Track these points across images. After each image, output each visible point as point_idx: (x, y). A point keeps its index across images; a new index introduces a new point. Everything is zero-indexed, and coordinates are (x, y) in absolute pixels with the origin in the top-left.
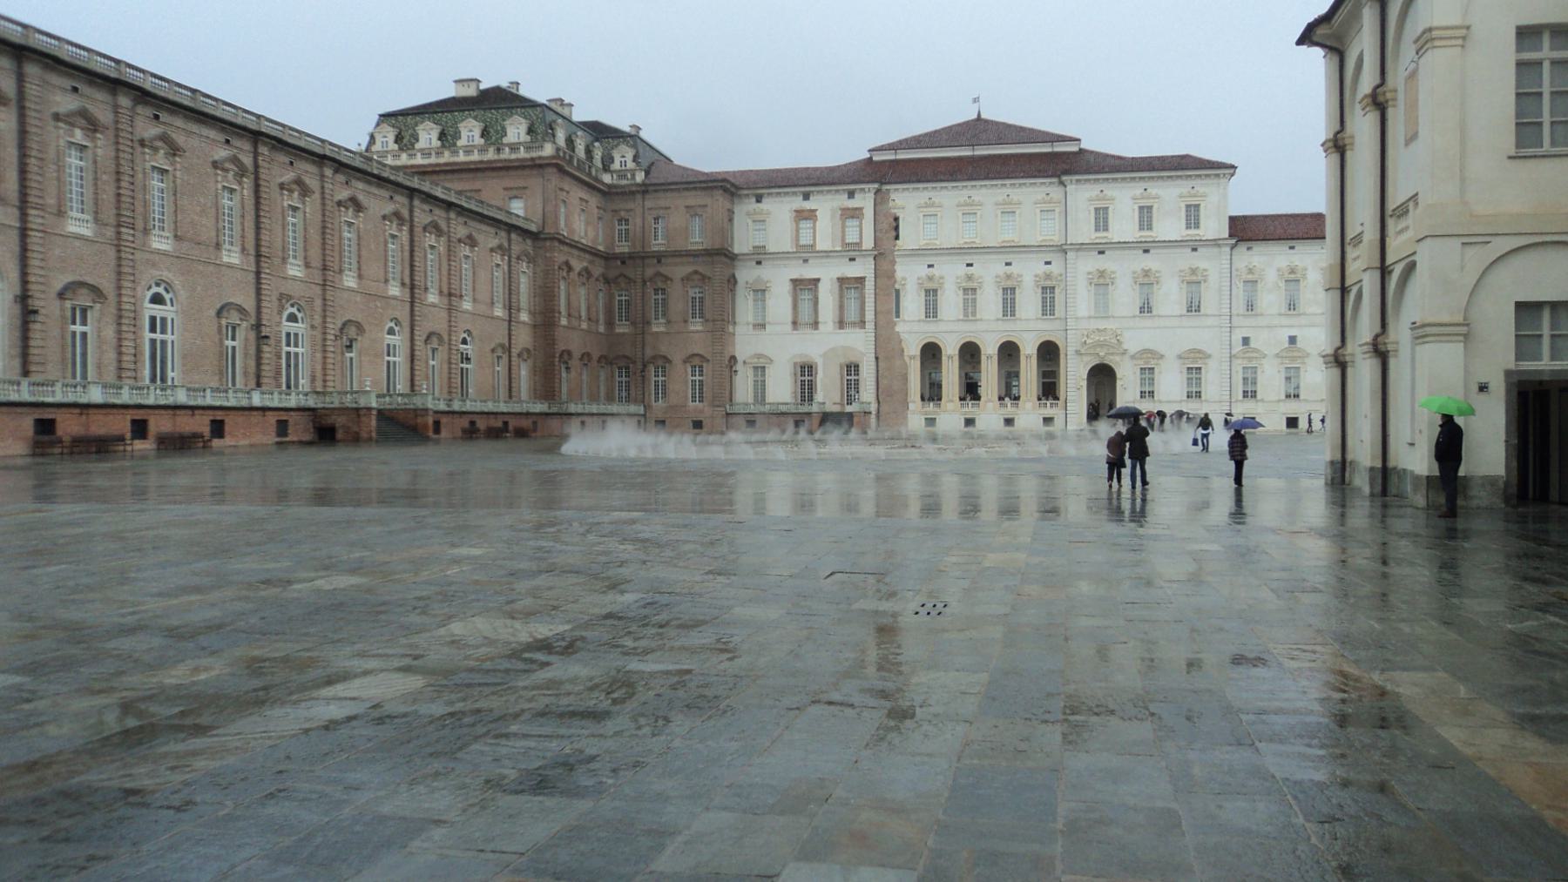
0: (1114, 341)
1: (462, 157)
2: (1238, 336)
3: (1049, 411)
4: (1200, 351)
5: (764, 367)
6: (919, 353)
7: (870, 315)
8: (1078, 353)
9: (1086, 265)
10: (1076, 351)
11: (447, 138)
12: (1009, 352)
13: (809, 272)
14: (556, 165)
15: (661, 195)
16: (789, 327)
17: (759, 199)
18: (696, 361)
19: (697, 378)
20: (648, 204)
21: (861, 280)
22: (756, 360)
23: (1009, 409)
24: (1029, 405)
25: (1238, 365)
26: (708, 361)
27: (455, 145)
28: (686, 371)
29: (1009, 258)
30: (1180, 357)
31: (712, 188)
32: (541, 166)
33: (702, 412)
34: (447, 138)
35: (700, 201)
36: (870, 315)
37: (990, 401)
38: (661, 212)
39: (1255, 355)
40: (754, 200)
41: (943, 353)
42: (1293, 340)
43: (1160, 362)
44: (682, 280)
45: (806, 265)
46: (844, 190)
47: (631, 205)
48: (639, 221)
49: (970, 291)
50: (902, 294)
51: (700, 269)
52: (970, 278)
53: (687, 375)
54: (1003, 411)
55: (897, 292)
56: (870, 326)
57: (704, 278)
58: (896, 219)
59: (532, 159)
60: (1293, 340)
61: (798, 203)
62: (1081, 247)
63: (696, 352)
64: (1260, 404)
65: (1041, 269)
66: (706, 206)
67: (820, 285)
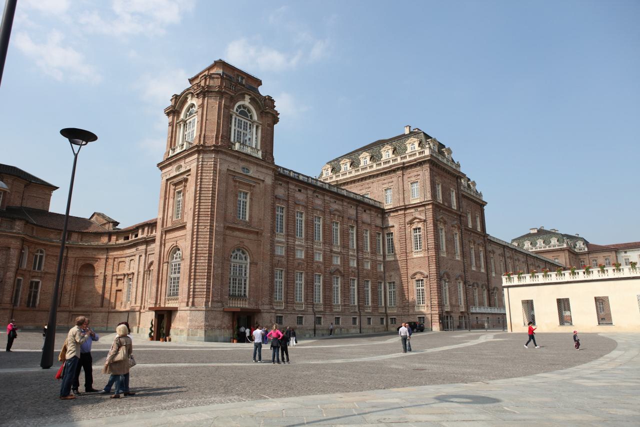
1: (539, 250)
11: (533, 244)
14: (568, 250)
15: (594, 254)
17: (626, 252)
20: (590, 256)
27: (536, 246)
31: (611, 251)
32: (564, 250)
34: (533, 244)
35: (609, 254)
38: (596, 259)
40: (624, 253)
47: (584, 257)
48: (588, 261)
59: (561, 248)
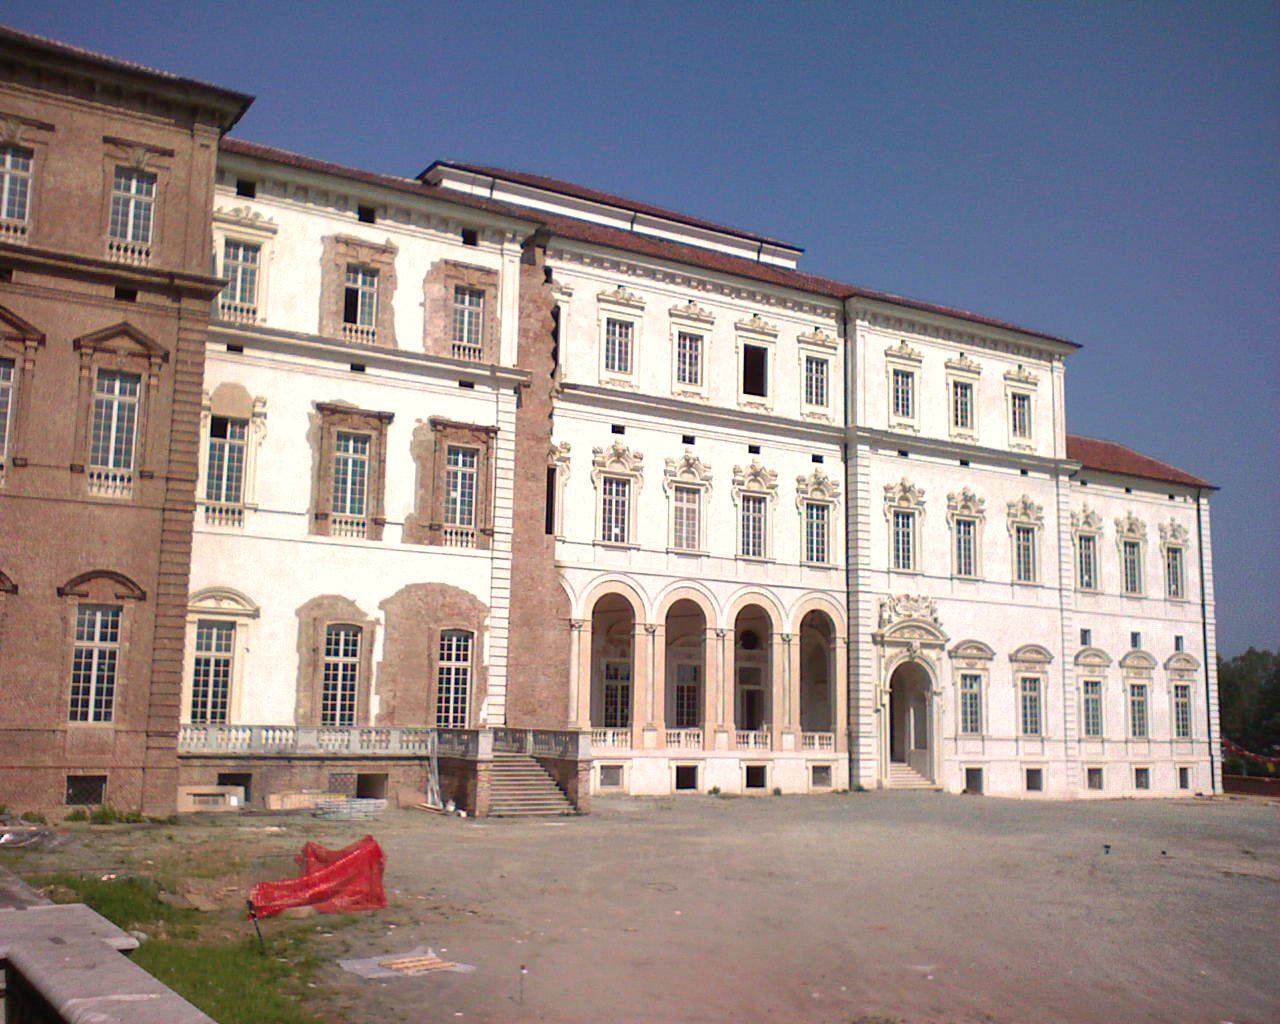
0: (930, 619)
2: (1077, 624)
3: (820, 754)
4: (1038, 650)
5: (232, 625)
6: (589, 617)
7: (503, 522)
8: (878, 640)
9: (879, 471)
10: (874, 636)
12: (686, 620)
13: (364, 393)
16: (304, 523)
18: (104, 591)
19: (97, 645)
21: (490, 432)
22: (210, 604)
23: (753, 753)
24: (789, 740)
25: (1083, 674)
26: (142, 597)
28: (65, 620)
29: (757, 438)
30: (1012, 659)
33: (102, 749)
36: (503, 522)
37: (720, 730)
39: (1097, 660)
41: (638, 619)
42: (1135, 637)
43: (989, 664)
44: (77, 345)
45: (358, 375)
46: (459, 223)
49: (687, 490)
50: (559, 480)
51: (137, 322)
52: (689, 465)
53: (65, 633)
54: (807, 754)
55: (551, 473)
56: (503, 543)
57: (148, 349)
58: (556, 314)
60: (1135, 637)
61: (348, 225)
62: (879, 440)
63: (101, 564)
64: (1106, 745)
65: (809, 469)
66: (170, 154)
67: (392, 431)
